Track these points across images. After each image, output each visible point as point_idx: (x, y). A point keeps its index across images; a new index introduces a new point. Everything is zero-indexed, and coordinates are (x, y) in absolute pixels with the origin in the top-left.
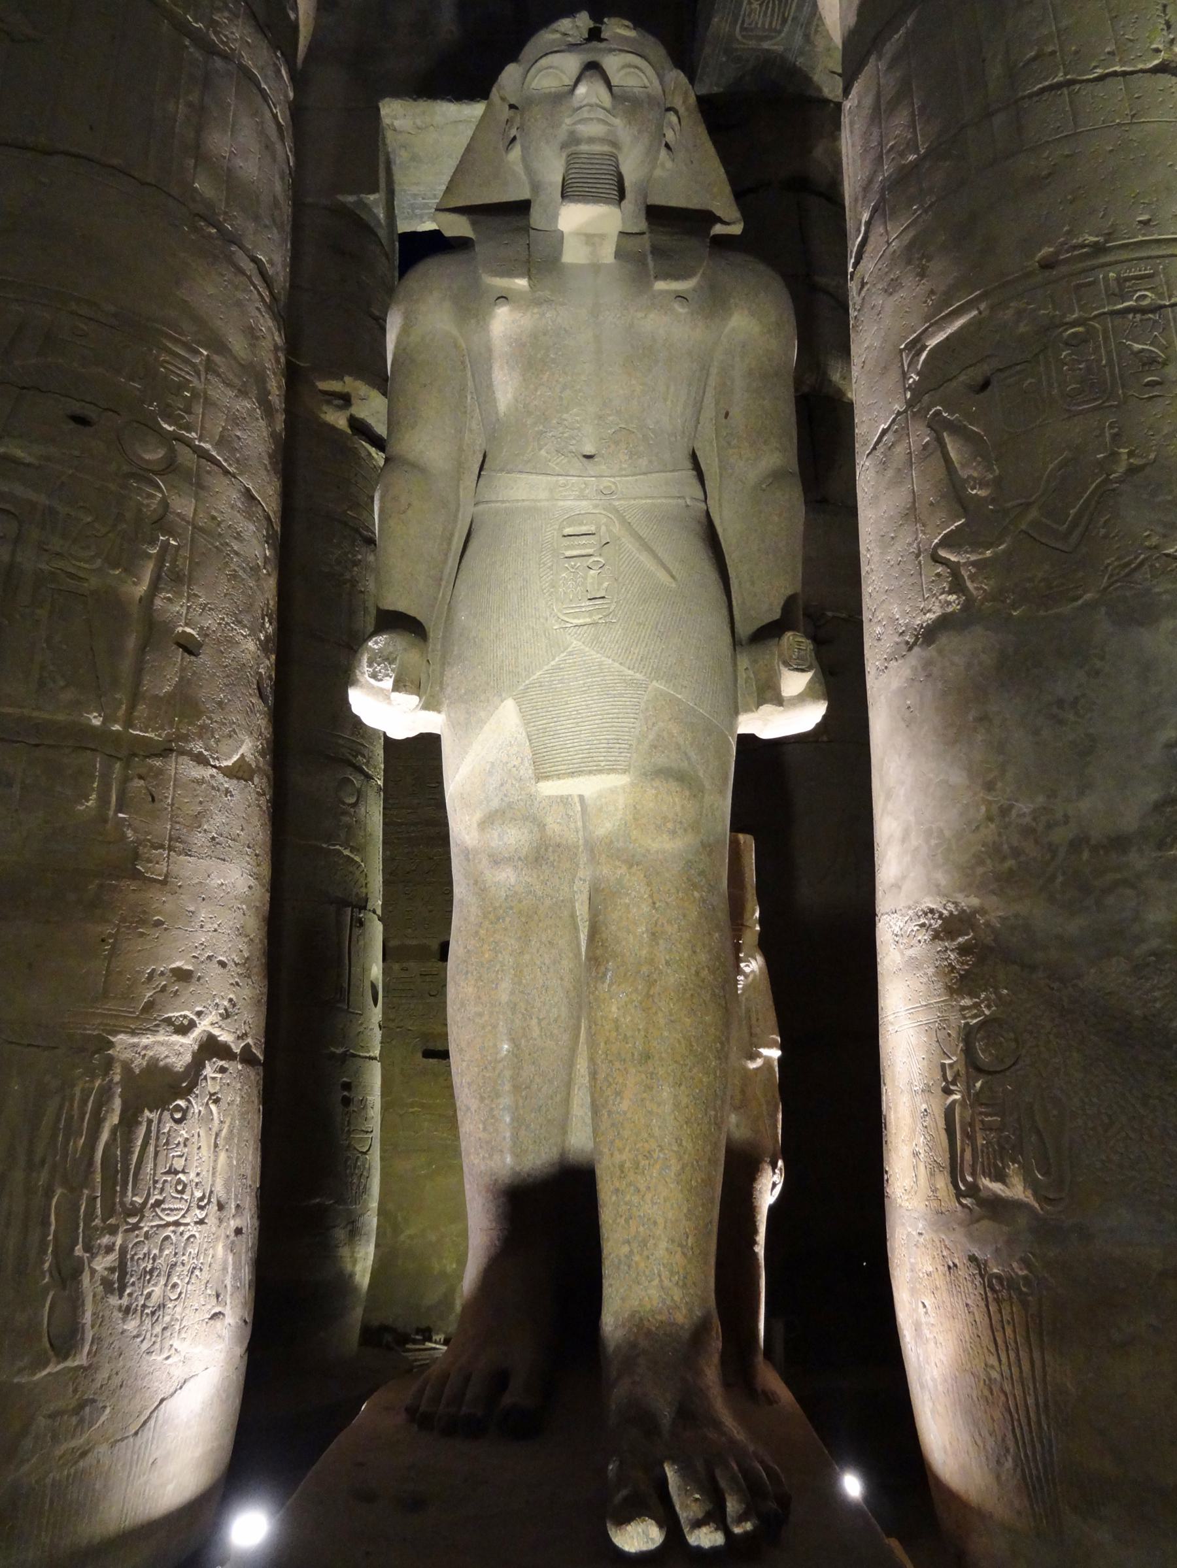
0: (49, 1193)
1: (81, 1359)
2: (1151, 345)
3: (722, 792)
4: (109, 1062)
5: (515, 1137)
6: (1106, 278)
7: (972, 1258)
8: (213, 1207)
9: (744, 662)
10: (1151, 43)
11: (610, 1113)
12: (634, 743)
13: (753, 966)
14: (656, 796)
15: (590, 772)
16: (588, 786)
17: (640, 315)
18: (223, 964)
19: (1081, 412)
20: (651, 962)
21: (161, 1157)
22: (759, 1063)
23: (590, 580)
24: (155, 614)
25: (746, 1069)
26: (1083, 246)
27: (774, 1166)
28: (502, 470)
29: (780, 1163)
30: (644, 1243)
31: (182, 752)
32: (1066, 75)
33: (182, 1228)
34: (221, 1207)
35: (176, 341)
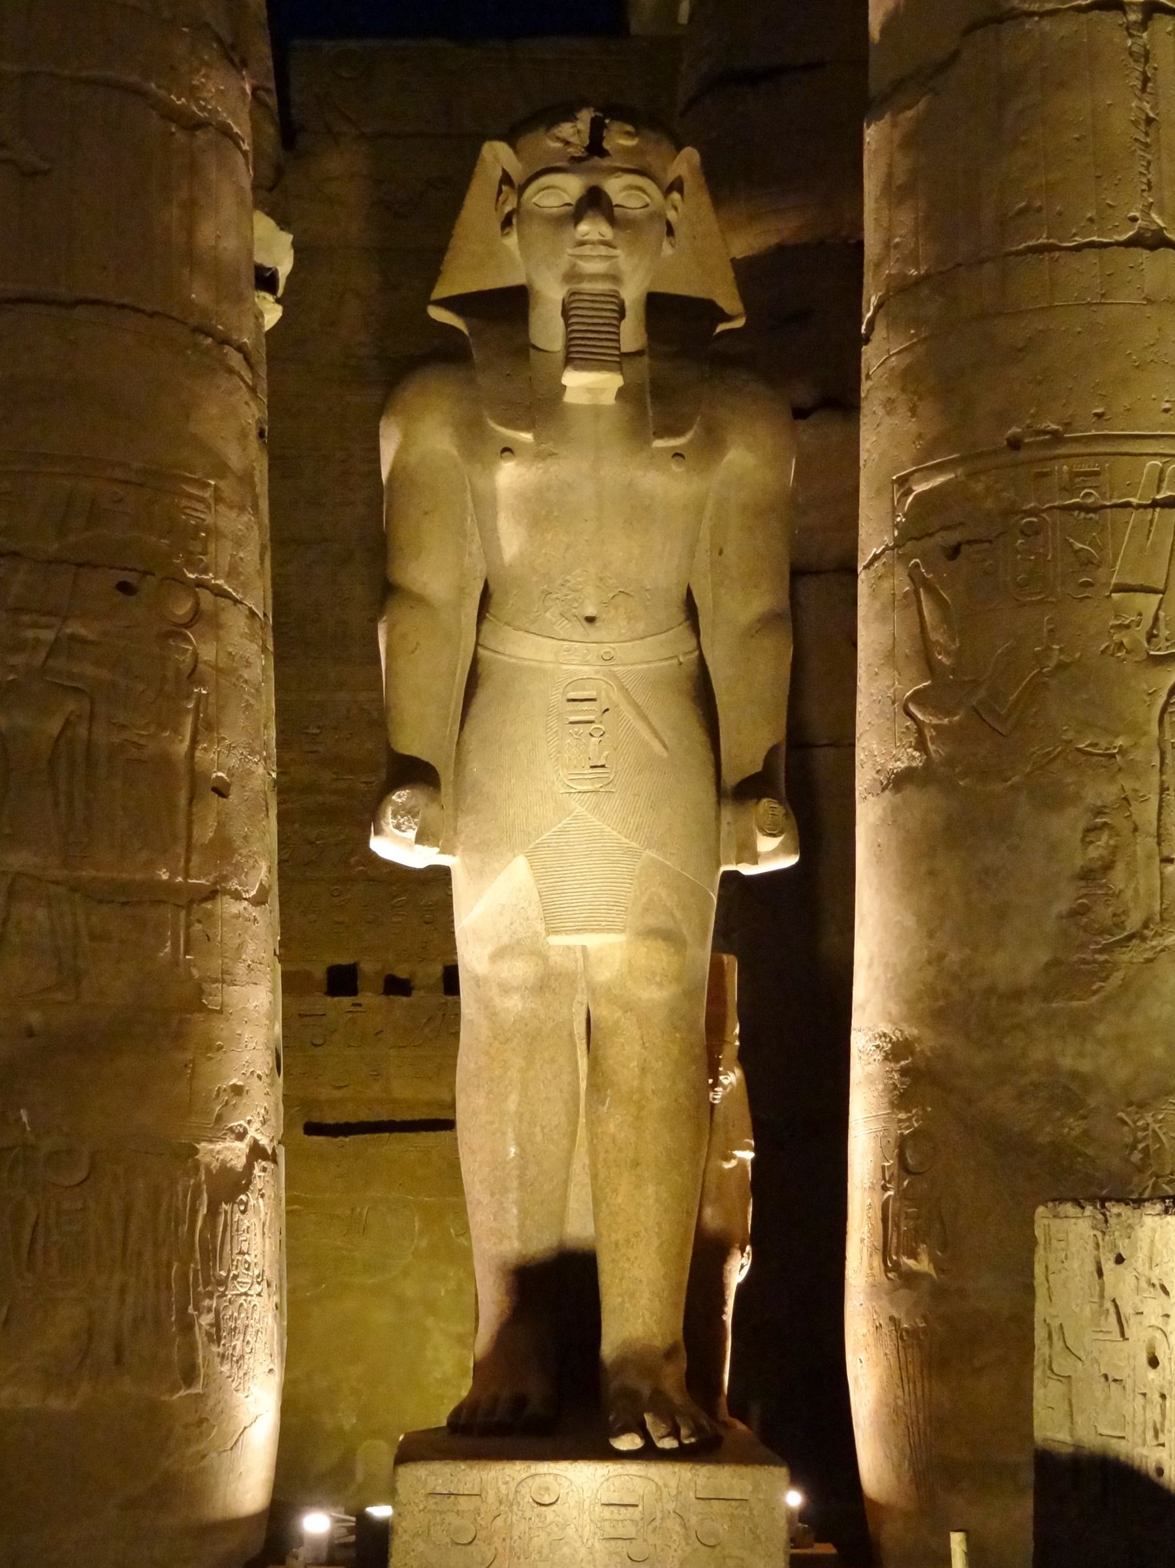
0: (169, 1266)
1: (198, 1389)
2: (1089, 545)
3: (702, 945)
4: (197, 1166)
5: (522, 1226)
6: (1061, 469)
7: (892, 1319)
8: (265, 1284)
9: (727, 814)
10: (1130, 210)
11: (608, 1205)
12: (630, 906)
13: (732, 1078)
14: (647, 953)
15: (593, 930)
16: (592, 941)
17: (640, 473)
18: (259, 1077)
19: (1032, 603)
20: (641, 1090)
21: (235, 1241)
22: (733, 1163)
23: (591, 748)
24: (196, 767)
25: (721, 1169)
26: (1045, 432)
27: (743, 1250)
28: (507, 624)
29: (748, 1248)
30: (632, 1295)
31: (226, 892)
32: (1048, 238)
33: (249, 1298)
34: (269, 1285)
35: (188, 481)
